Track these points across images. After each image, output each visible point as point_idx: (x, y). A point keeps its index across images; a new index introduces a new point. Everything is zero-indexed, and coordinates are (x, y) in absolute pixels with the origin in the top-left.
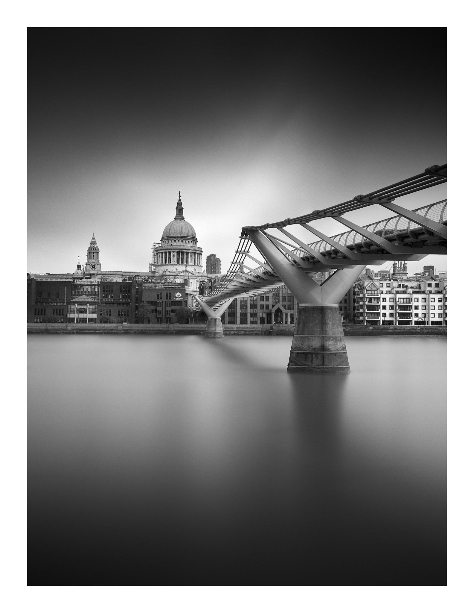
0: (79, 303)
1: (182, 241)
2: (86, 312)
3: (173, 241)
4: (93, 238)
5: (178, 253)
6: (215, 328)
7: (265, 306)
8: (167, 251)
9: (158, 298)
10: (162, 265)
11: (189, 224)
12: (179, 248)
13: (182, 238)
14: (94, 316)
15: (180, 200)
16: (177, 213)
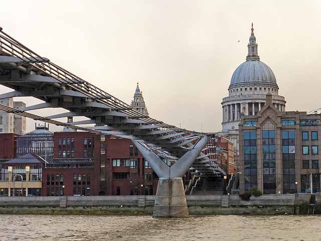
0: (15, 166)
1: (256, 89)
2: (25, 179)
3: (244, 89)
4: (138, 90)
5: (250, 104)
6: (170, 198)
7: (310, 162)
8: (235, 103)
9: (131, 154)
10: (229, 122)
11: (266, 66)
12: (251, 98)
13: (255, 84)
14: (37, 185)
15: (252, 34)
16: (249, 50)
